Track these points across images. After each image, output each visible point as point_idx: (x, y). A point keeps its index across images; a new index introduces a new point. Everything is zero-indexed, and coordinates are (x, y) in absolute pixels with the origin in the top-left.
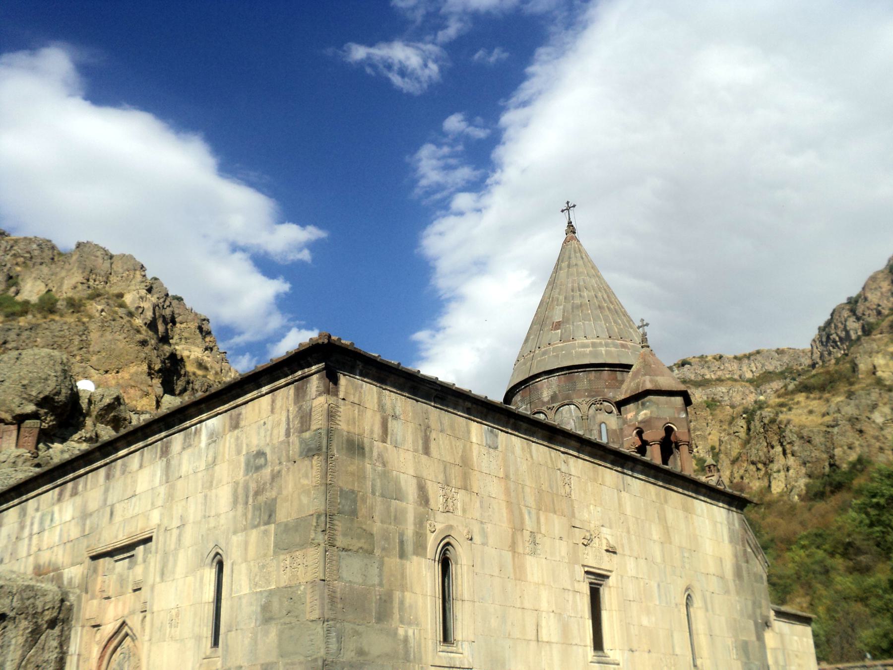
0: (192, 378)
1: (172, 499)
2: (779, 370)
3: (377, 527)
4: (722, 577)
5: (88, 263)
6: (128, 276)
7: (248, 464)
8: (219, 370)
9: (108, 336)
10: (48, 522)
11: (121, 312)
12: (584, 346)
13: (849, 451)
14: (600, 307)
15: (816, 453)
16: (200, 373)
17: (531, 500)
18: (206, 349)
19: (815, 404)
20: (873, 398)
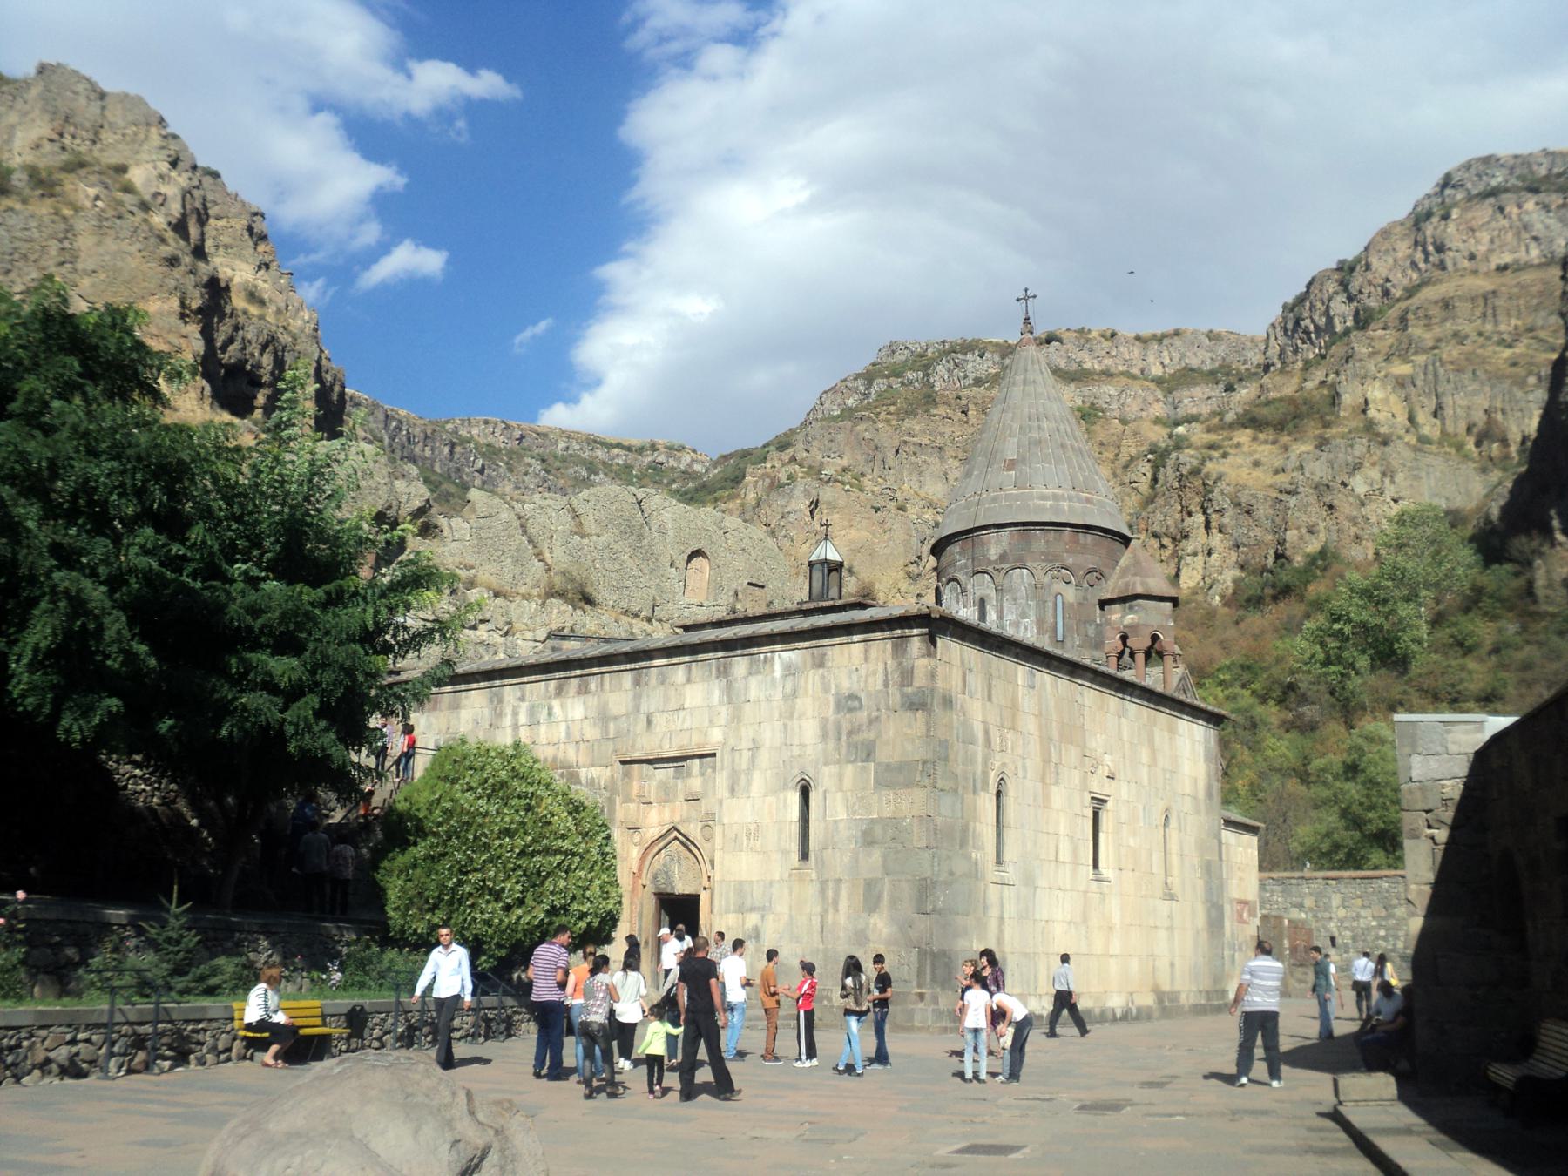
0: (241, 320)
1: (739, 721)
2: (1208, 367)
3: (959, 769)
4: (1195, 798)
5: (59, 103)
6: (135, 134)
7: (839, 706)
8: (283, 305)
9: (111, 245)
10: (543, 715)
11: (128, 199)
12: (1044, 497)
13: (1307, 536)
14: (1063, 446)
15: (1258, 532)
16: (254, 310)
17: (1055, 734)
18: (260, 268)
19: (1265, 451)
20: (1357, 453)
